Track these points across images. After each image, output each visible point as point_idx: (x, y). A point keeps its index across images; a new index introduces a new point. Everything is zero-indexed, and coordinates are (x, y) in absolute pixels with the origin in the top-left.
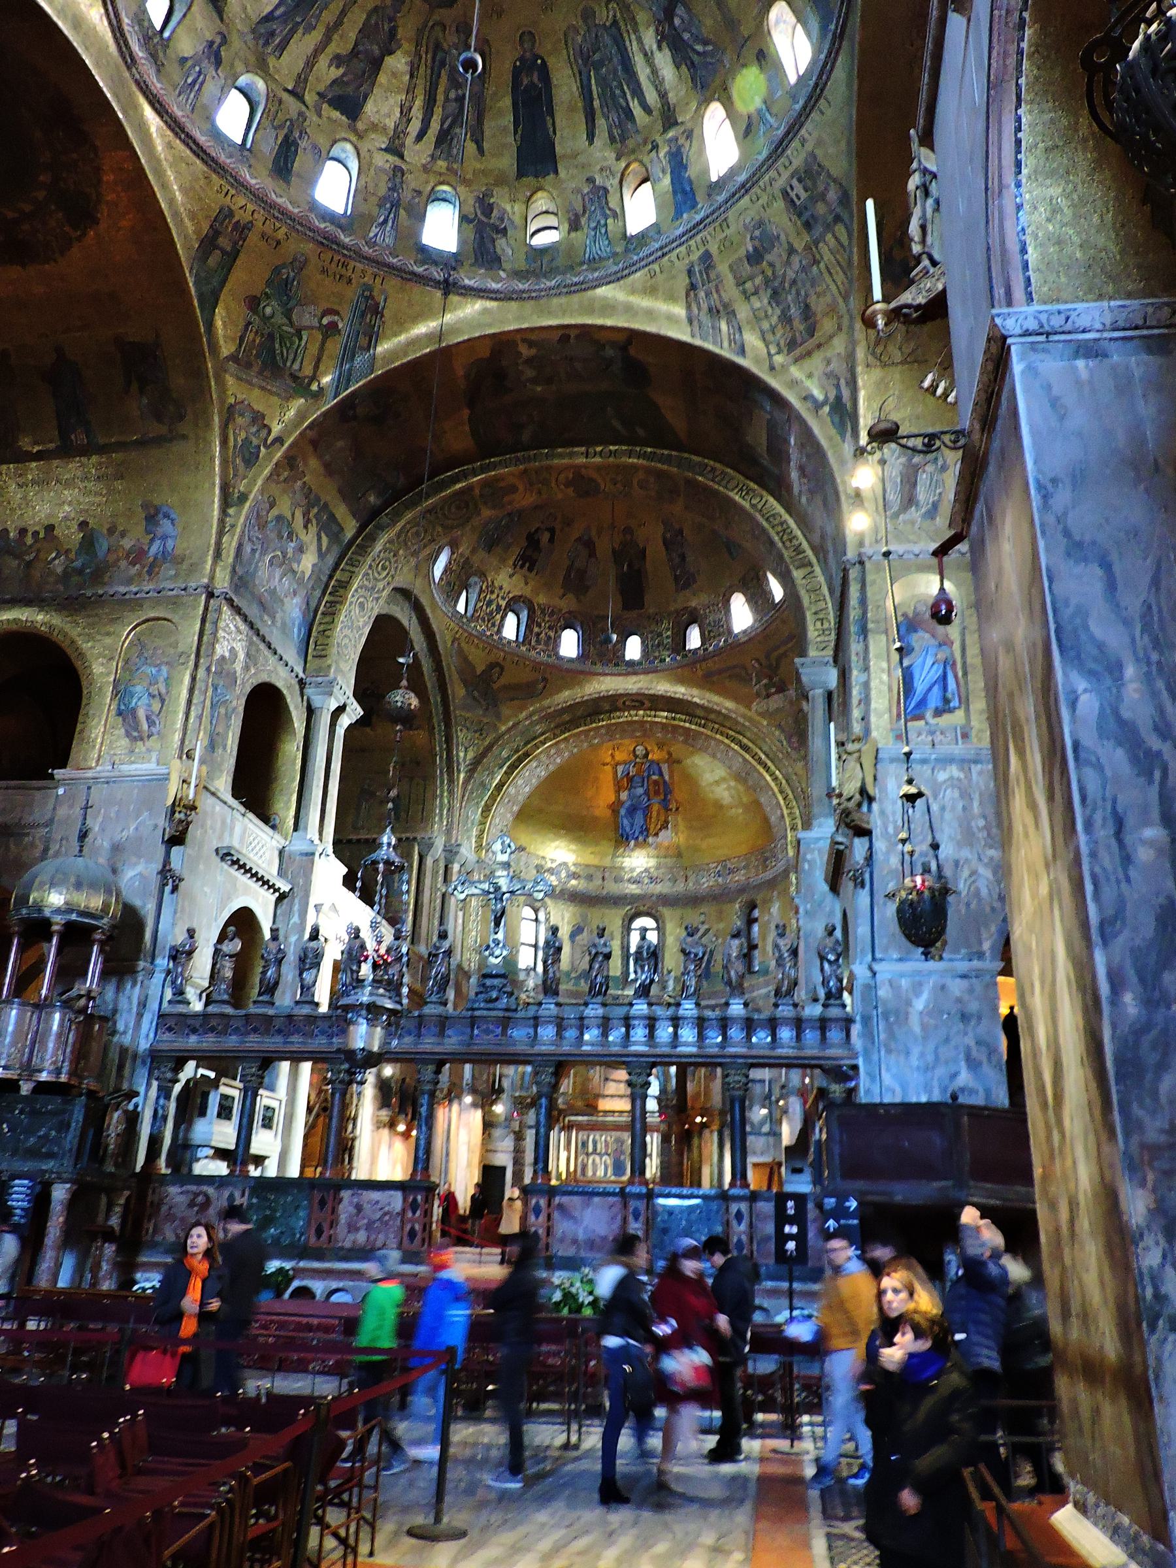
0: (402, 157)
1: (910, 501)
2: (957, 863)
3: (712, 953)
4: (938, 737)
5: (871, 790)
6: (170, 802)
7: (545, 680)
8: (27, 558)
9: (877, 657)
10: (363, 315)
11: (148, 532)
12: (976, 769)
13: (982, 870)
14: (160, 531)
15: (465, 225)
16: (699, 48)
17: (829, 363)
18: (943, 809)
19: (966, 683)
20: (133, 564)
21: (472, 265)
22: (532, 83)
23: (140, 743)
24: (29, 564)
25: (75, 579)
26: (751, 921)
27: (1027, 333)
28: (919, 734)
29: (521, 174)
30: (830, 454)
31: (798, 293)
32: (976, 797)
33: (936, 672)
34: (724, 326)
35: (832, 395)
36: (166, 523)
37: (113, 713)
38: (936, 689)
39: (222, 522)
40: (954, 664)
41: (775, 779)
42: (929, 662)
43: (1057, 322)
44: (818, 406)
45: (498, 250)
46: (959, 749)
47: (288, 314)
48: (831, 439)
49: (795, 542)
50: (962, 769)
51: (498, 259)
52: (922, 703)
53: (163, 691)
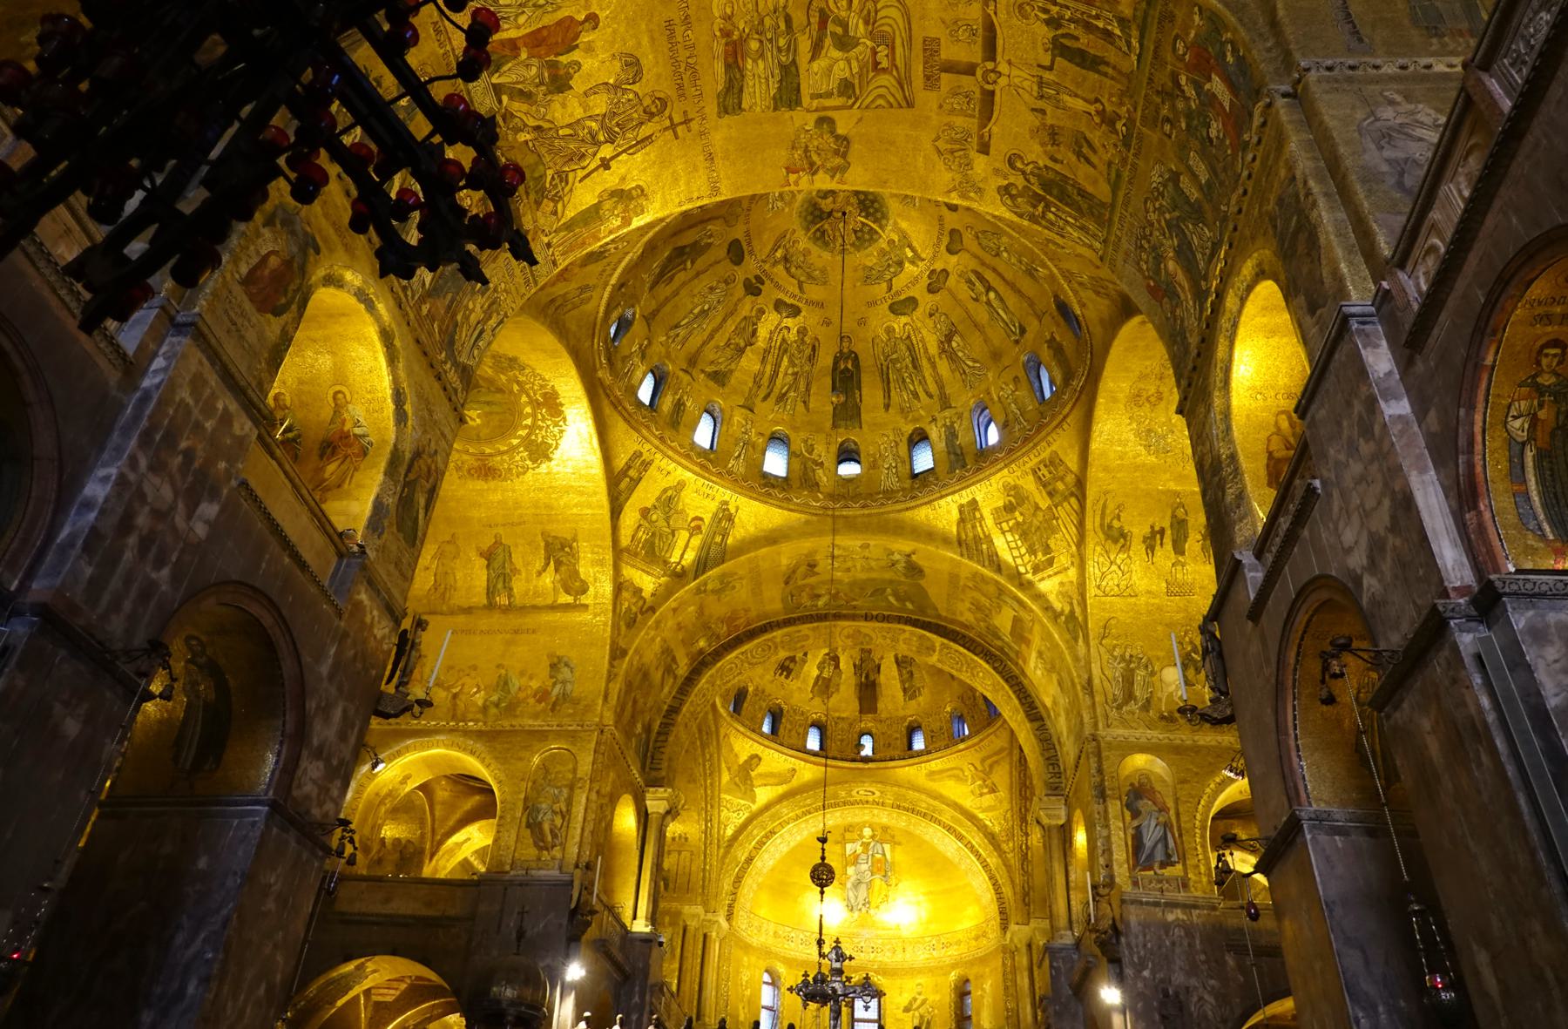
0: (752, 411)
1: (1129, 696)
2: (1187, 988)
5: (1120, 926)
6: (573, 906)
7: (794, 770)
8: (454, 691)
9: (1115, 818)
11: (551, 677)
12: (1195, 912)
13: (1206, 997)
14: (560, 677)
15: (793, 459)
16: (970, 364)
18: (1173, 944)
19: (1182, 843)
20: (539, 701)
22: (847, 368)
23: (545, 852)
24: (455, 696)
25: (493, 711)
27: (1310, 819)
28: (1151, 882)
29: (835, 426)
31: (1042, 536)
32: (1198, 935)
33: (1159, 832)
35: (1067, 610)
36: (566, 670)
37: (524, 824)
38: (1160, 846)
39: (609, 672)
40: (1172, 826)
42: (1153, 823)
43: (1325, 816)
44: (1056, 616)
46: (1181, 896)
47: (667, 520)
48: (1067, 642)
49: (1029, 700)
50: (1184, 913)
51: (817, 484)
52: (1151, 856)
53: (564, 809)
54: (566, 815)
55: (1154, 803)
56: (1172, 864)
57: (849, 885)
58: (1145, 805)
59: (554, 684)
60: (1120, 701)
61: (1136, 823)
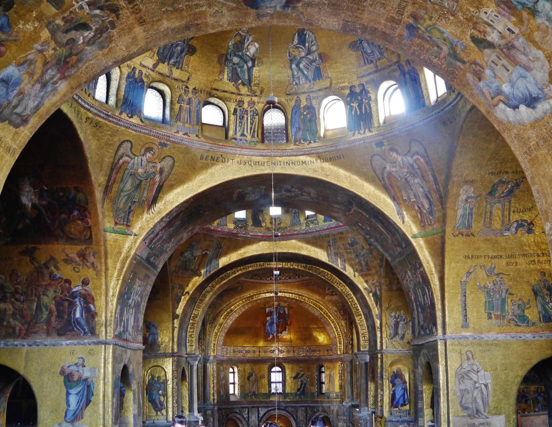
3: (305, 384)
4: (402, 414)
7: (242, 286)
10: (216, 249)
11: (147, 332)
17: (373, 280)
21: (252, 226)
23: (159, 412)
26: (321, 372)
30: (373, 311)
34: (339, 261)
35: (374, 290)
41: (333, 322)
42: (400, 388)
45: (261, 218)
46: (407, 418)
48: (373, 305)
50: (407, 424)
52: (398, 402)
54: (165, 395)
55: (402, 380)
56: (405, 405)
57: (267, 324)
58: (398, 381)
59: (149, 335)
60: (392, 336)
61: (393, 389)
